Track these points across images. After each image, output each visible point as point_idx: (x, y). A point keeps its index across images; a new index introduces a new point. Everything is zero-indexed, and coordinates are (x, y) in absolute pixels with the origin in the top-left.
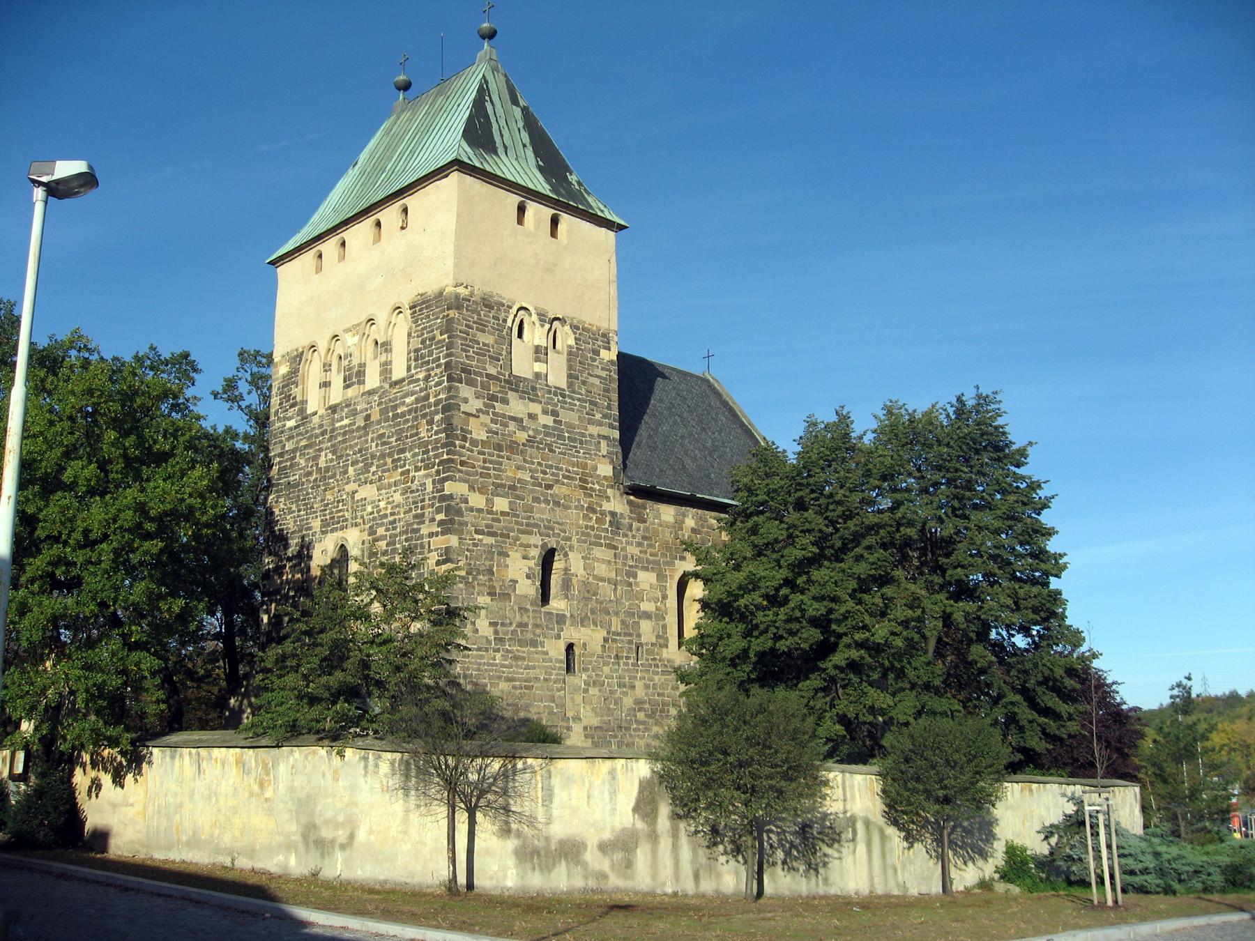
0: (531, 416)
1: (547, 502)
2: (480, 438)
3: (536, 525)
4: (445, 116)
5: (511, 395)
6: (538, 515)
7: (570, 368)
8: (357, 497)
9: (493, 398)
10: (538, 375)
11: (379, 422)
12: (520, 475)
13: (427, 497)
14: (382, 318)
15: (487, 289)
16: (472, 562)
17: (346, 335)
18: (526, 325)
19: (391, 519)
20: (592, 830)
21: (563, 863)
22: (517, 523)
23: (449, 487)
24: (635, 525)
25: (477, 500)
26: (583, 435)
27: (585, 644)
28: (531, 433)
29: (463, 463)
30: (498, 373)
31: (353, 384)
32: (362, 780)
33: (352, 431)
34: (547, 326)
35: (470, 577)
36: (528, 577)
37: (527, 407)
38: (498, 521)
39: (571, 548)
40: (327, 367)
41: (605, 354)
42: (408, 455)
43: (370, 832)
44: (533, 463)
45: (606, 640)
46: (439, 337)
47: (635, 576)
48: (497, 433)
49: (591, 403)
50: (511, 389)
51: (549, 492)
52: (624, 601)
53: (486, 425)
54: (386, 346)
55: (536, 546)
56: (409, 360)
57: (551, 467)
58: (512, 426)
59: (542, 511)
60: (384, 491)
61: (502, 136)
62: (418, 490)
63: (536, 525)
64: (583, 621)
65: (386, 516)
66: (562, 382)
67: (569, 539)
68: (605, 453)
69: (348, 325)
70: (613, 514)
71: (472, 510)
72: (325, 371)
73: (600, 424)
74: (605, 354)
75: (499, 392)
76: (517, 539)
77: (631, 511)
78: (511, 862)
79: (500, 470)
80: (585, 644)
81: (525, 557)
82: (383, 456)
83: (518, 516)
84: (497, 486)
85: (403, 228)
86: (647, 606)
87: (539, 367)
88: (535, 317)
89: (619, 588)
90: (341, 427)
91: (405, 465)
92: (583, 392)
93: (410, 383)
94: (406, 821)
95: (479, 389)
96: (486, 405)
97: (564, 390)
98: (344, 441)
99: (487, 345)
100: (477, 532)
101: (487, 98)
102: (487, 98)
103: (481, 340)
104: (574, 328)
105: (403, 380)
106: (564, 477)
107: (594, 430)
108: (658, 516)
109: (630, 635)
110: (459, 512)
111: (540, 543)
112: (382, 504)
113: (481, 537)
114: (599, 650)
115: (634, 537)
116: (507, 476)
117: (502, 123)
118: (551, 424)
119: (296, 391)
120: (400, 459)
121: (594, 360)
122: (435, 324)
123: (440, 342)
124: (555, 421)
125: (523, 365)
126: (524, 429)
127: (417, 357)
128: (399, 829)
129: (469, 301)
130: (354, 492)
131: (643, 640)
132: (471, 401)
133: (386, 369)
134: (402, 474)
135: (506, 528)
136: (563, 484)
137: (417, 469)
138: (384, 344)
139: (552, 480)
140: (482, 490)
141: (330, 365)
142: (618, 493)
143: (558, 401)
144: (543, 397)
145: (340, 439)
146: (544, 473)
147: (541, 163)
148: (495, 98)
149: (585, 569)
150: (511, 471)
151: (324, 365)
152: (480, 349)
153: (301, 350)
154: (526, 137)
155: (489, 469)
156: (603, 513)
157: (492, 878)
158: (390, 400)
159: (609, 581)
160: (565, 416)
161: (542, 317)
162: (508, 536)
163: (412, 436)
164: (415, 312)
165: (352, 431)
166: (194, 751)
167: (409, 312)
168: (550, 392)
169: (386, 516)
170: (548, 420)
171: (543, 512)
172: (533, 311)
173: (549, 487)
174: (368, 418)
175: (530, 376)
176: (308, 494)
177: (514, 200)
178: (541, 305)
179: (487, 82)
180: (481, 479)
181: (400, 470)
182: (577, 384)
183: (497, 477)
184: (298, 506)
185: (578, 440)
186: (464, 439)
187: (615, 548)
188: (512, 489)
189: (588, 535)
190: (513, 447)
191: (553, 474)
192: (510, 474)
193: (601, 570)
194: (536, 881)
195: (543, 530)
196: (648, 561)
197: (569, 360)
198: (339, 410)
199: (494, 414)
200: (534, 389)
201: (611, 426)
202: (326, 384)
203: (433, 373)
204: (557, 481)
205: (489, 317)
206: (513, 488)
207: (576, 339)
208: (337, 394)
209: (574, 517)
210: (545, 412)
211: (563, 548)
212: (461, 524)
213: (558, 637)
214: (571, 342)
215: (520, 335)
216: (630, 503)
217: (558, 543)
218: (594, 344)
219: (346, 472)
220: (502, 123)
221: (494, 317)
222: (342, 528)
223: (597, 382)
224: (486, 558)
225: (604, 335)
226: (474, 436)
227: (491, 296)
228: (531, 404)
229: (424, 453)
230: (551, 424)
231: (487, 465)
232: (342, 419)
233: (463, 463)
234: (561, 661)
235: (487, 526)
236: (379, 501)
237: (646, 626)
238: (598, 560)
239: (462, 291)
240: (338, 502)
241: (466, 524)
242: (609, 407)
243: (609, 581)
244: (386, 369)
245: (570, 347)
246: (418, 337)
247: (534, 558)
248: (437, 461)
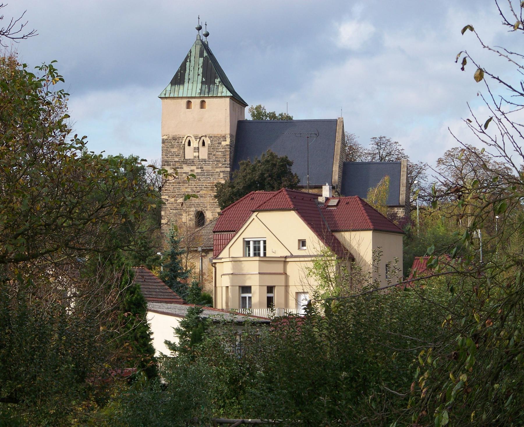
0: (191, 171)
3: (193, 205)
5: (184, 166)
10: (195, 157)
12: (187, 190)
15: (174, 134)
26: (213, 173)
29: (166, 190)
34: (198, 140)
37: (190, 168)
39: (207, 210)
41: (224, 143)
49: (217, 161)
57: (199, 185)
61: (189, 74)
63: (193, 205)
66: (206, 157)
71: (169, 203)
73: (220, 167)
74: (224, 143)
79: (179, 190)
87: (196, 154)
88: (193, 138)
99: (175, 152)
100: (171, 209)
102: (188, 60)
103: (172, 151)
106: (204, 188)
107: (218, 170)
117: (192, 68)
121: (219, 146)
124: (201, 170)
125: (190, 154)
136: (204, 190)
147: (204, 80)
148: (192, 58)
154: (201, 70)
160: (205, 167)
161: (196, 137)
170: (199, 171)
173: (199, 192)
175: (192, 158)
177: (186, 100)
178: (196, 133)
183: (178, 192)
191: (200, 188)
192: (183, 190)
197: (208, 149)
201: (226, 167)
204: (201, 190)
207: (211, 141)
210: (197, 168)
212: (165, 208)
214: (209, 142)
215: (189, 144)
217: (202, 209)
221: (177, 143)
223: (220, 153)
225: (223, 137)
228: (192, 167)
231: (175, 189)
233: (166, 190)
239: (165, 137)
241: (167, 208)
242: (225, 161)
245: (209, 144)
247: (192, 215)
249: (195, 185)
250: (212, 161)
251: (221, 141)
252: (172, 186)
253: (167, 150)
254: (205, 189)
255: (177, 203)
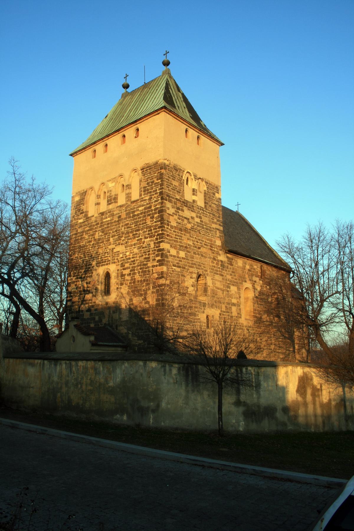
0: (192, 218)
1: (198, 254)
2: (174, 225)
3: (195, 264)
4: (150, 94)
5: (185, 208)
6: (195, 260)
7: (205, 199)
8: (115, 251)
9: (178, 209)
10: (194, 201)
11: (126, 219)
13: (151, 250)
14: (126, 175)
15: (176, 163)
16: (172, 279)
17: (109, 183)
18: (189, 180)
19: (133, 260)
20: (279, 402)
21: (266, 418)
22: (188, 263)
23: (163, 246)
24: (229, 266)
25: (173, 252)
26: (211, 228)
27: (213, 316)
28: (192, 225)
29: (168, 235)
30: (180, 198)
31: (112, 203)
32: (163, 377)
33: (112, 223)
35: (171, 285)
36: (192, 286)
38: (181, 261)
40: (98, 197)
42: (141, 232)
43: (168, 403)
44: (193, 238)
45: (220, 314)
46: (156, 181)
47: (230, 288)
48: (180, 224)
50: (185, 206)
51: (199, 250)
52: (226, 298)
53: (176, 220)
54: (129, 186)
55: (195, 273)
56: (141, 191)
57: (199, 240)
58: (186, 221)
59: (197, 258)
60: (128, 248)
62: (146, 247)
63: (195, 264)
64: (212, 306)
65: (130, 258)
67: (206, 271)
68: (218, 236)
69: (109, 179)
70: (222, 261)
71: (171, 256)
72: (98, 198)
73: (216, 224)
75: (180, 206)
76: (188, 270)
77: (228, 261)
78: (241, 418)
79: (181, 239)
80: (213, 316)
81: (191, 278)
82: (128, 233)
83: (188, 260)
84: (181, 246)
85: (136, 137)
86: (234, 301)
87: (194, 198)
88: (193, 177)
89: (224, 292)
90: (106, 221)
91: (139, 236)
92: (210, 210)
93: (141, 201)
94: (187, 398)
95: (173, 204)
96: (176, 211)
97: (203, 208)
98: (108, 227)
100: (174, 265)
101: (169, 87)
104: (206, 183)
105: (138, 200)
106: (205, 245)
107: (214, 226)
108: (237, 263)
109: (228, 312)
110: (167, 256)
111: (196, 272)
112: (128, 254)
113: (175, 268)
114: (218, 318)
115: (229, 271)
116: (184, 242)
118: (199, 222)
119: (83, 207)
120: (137, 234)
122: (154, 176)
123: (156, 183)
124: (201, 221)
126: (190, 223)
127: (145, 190)
128: (183, 402)
129: (169, 166)
130: (113, 249)
131: (233, 315)
132: (170, 209)
133: (128, 196)
134: (138, 240)
135: (184, 264)
137: (146, 238)
138: (127, 186)
139: (200, 245)
140: (175, 248)
141: (100, 196)
142: (223, 253)
143: (202, 212)
144: (196, 210)
145: (106, 226)
146: (197, 242)
147: (191, 115)
149: (212, 284)
150: (186, 240)
151: (97, 196)
152: (173, 187)
153: (85, 190)
155: (177, 239)
156: (218, 261)
157: (232, 426)
158: (131, 209)
159: (221, 289)
162: (184, 268)
163: (143, 224)
164: (144, 171)
165: (112, 223)
166: (68, 362)
167: (141, 171)
168: (198, 208)
169: (130, 258)
170: (198, 220)
171: (197, 259)
172: (192, 174)
174: (120, 217)
175: (191, 201)
176: (90, 250)
178: (195, 172)
179: (168, 81)
180: (175, 243)
181: (137, 239)
182: (208, 206)
183: (181, 242)
184: (84, 255)
185: (209, 229)
186: (168, 225)
187: (222, 275)
188: (186, 248)
189: (213, 269)
190: (186, 230)
192: (185, 242)
193: (218, 284)
194: (254, 427)
195: (197, 266)
196: (234, 282)
197: (205, 196)
198: (105, 214)
199: (179, 215)
200: (193, 206)
201: (220, 225)
202: (98, 204)
203: (153, 197)
204: (202, 246)
205: (176, 174)
206: (186, 247)
207: (207, 188)
208: (104, 207)
209: (208, 262)
210: (197, 217)
211: (204, 275)
213: (204, 312)
214: (206, 189)
215: (187, 184)
216: (227, 257)
217: (203, 272)
218: (213, 190)
219: (109, 240)
220: (176, 98)
222: (107, 264)
223: (215, 206)
224: (177, 277)
225: (217, 187)
226: (172, 224)
227: (178, 166)
228: (192, 213)
229: (149, 231)
230: (199, 222)
231: (177, 237)
232: (106, 218)
233: (168, 235)
234: (205, 323)
235: (177, 263)
236: (126, 252)
237: (234, 309)
238: (217, 280)
240: (105, 253)
242: (219, 217)
243: (221, 289)
244: (128, 196)
245: (205, 190)
246: (145, 181)
247: (194, 278)
248: (156, 234)
249: (196, 238)
250: (209, 213)
251: (215, 192)
252: (175, 232)
253: (169, 181)
254: (205, 246)
255: (178, 257)
